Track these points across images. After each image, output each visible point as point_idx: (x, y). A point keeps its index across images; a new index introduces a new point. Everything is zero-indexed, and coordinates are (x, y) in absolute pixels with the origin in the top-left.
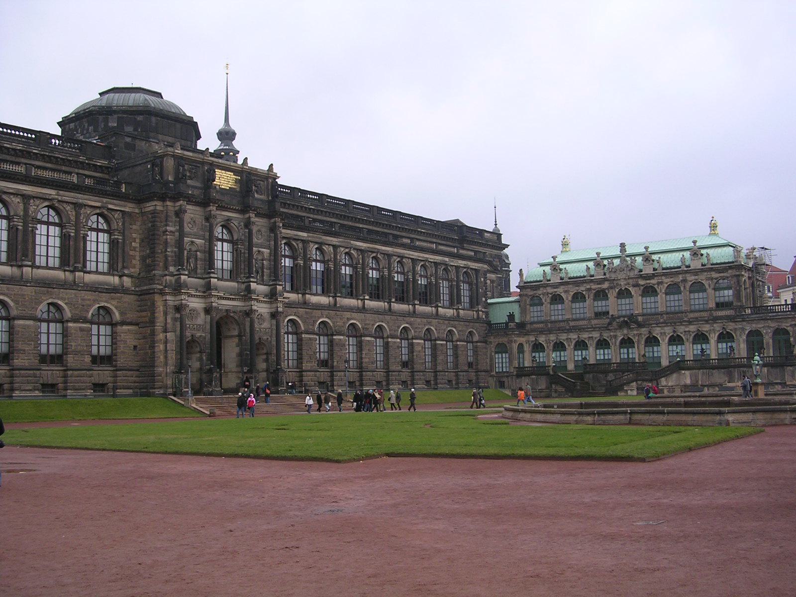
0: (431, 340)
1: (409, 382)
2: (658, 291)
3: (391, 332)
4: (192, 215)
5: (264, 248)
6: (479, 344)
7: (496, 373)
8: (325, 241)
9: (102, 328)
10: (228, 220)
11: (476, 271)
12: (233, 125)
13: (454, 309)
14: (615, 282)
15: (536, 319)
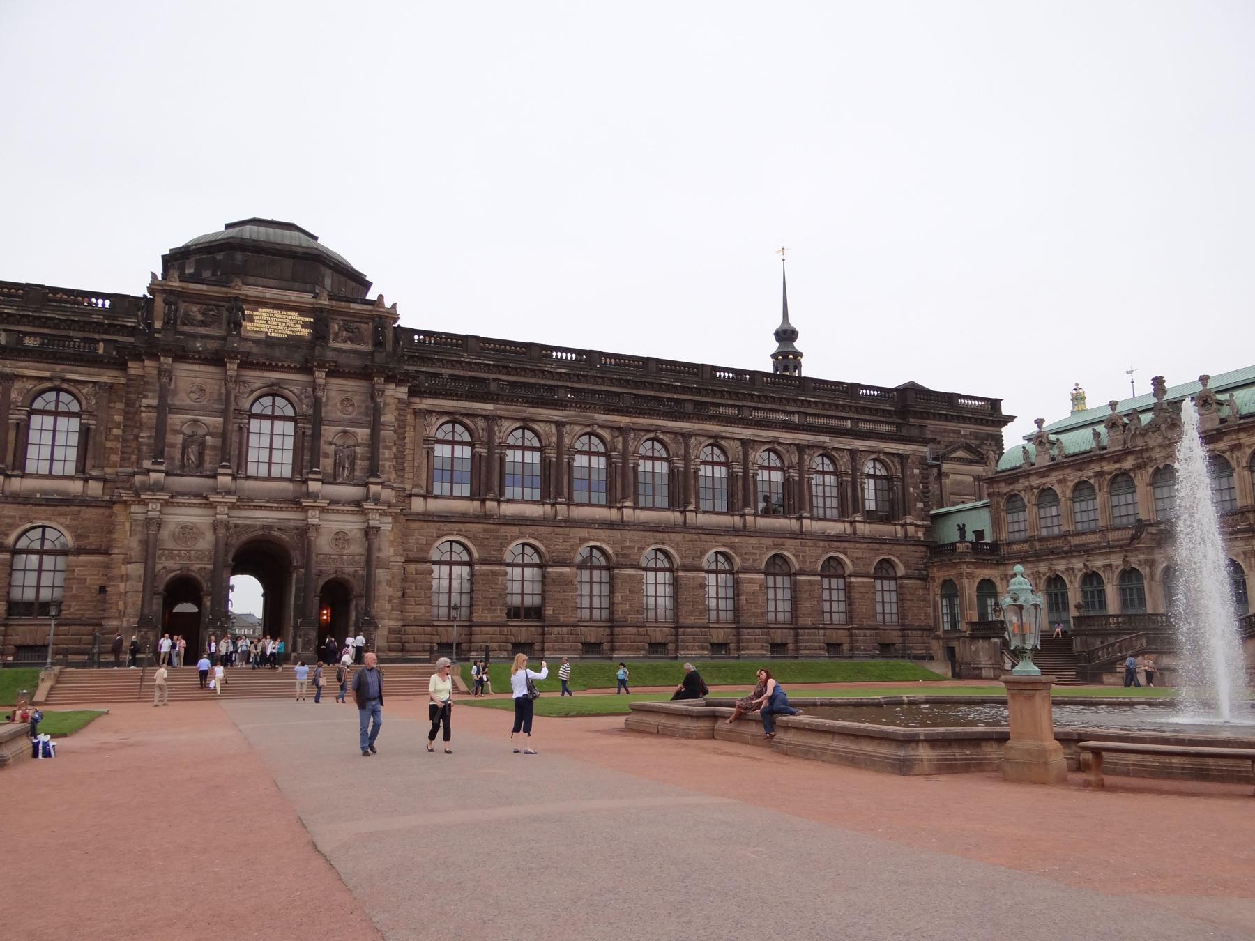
0: (789, 575)
1: (732, 646)
2: (1233, 463)
3: (684, 561)
4: (199, 380)
5: (358, 427)
6: (905, 581)
7: (945, 632)
8: (533, 416)
9: (779, 579)
10: (273, 384)
11: (902, 458)
12: (794, 322)
13: (844, 522)
14: (1146, 455)
15: (1017, 536)
